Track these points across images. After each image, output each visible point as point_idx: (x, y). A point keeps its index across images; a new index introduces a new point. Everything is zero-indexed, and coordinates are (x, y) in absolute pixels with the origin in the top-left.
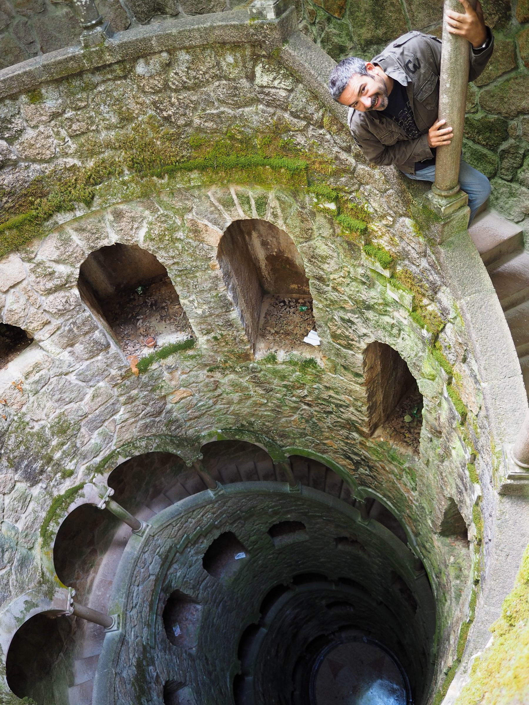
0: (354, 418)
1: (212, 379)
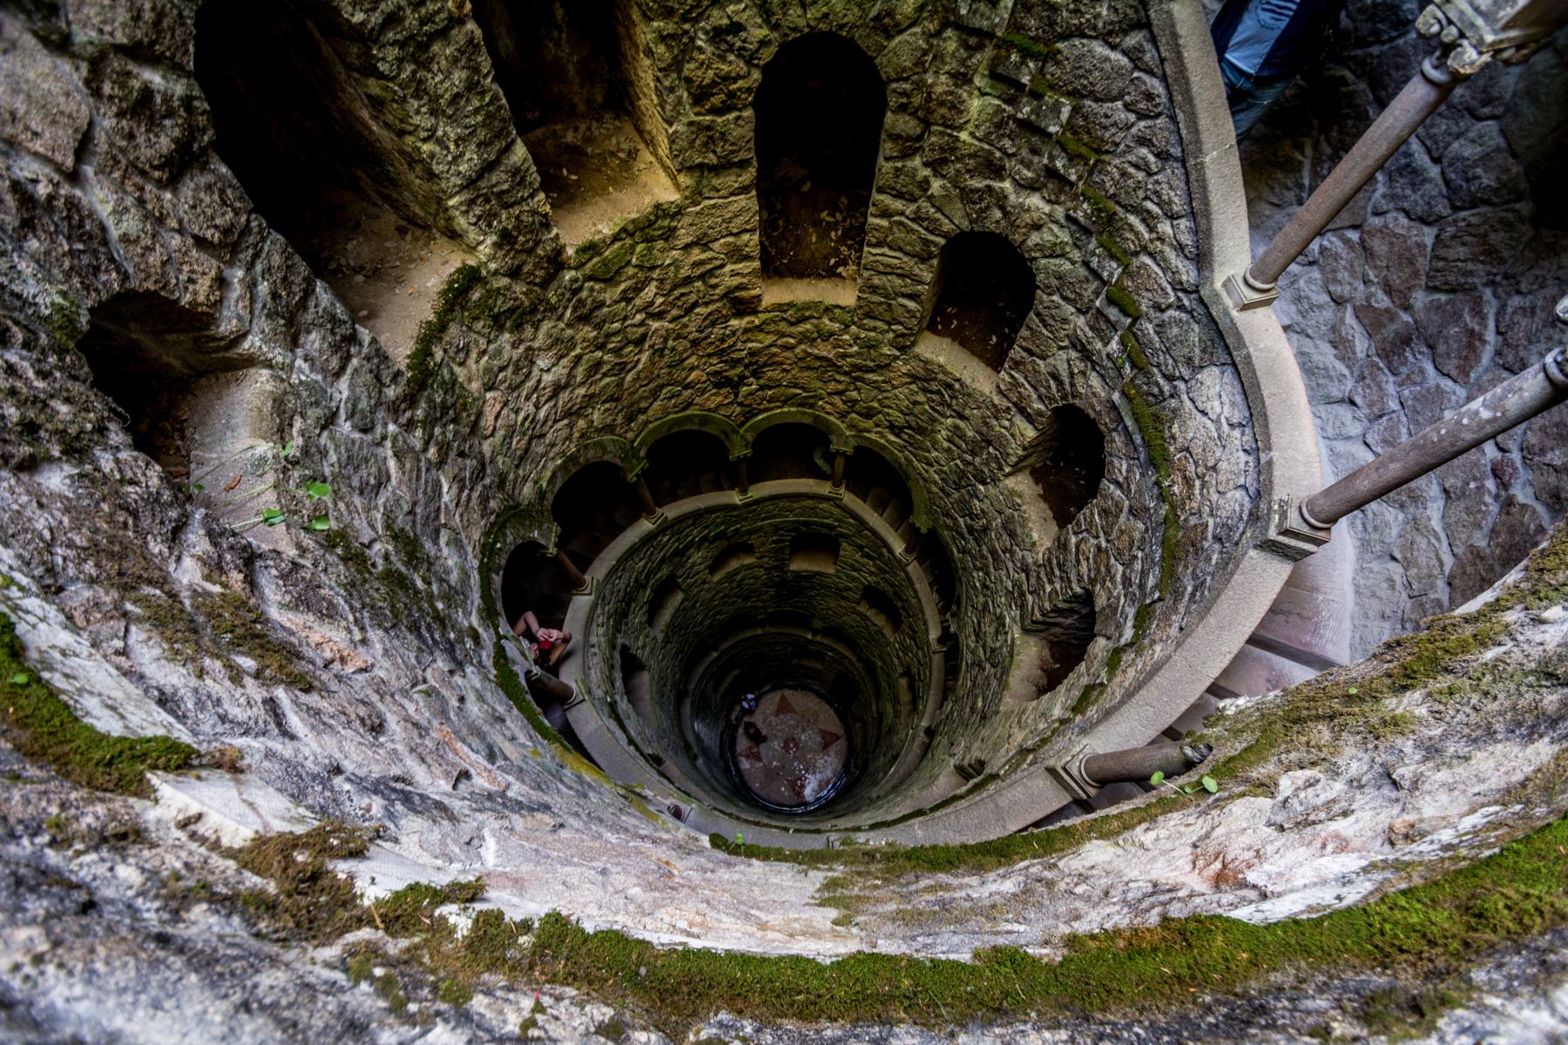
0: (737, 281)
1: (521, 349)
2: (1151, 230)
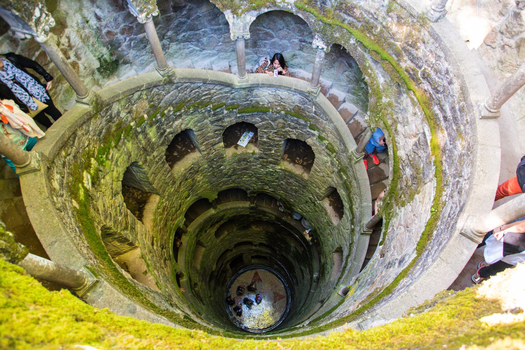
2: (210, 94)
